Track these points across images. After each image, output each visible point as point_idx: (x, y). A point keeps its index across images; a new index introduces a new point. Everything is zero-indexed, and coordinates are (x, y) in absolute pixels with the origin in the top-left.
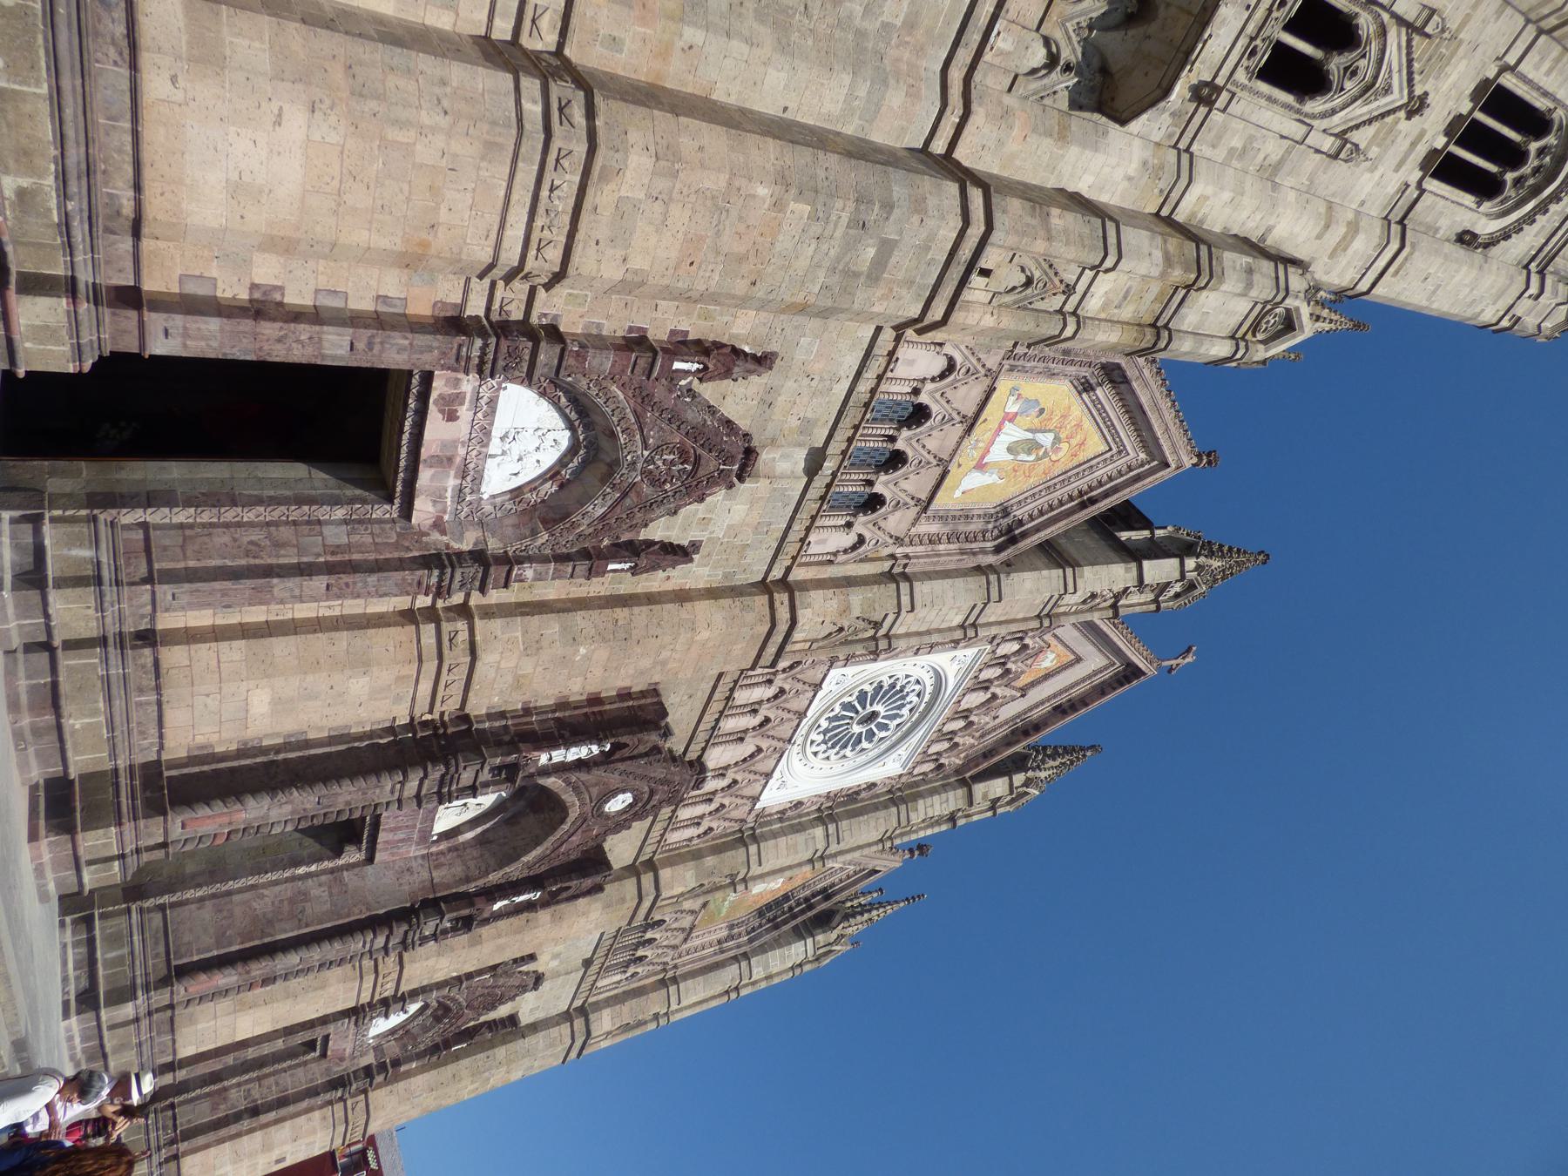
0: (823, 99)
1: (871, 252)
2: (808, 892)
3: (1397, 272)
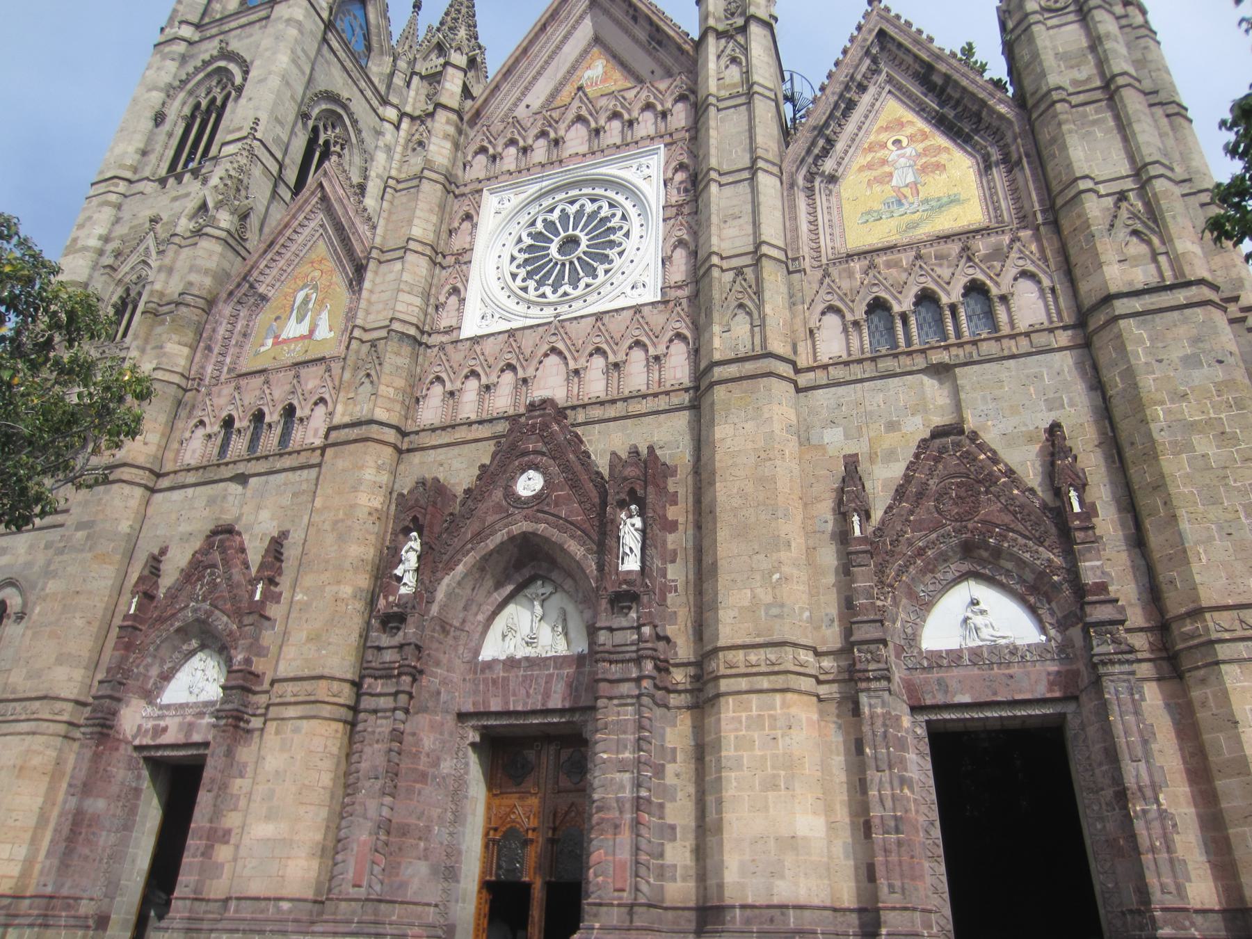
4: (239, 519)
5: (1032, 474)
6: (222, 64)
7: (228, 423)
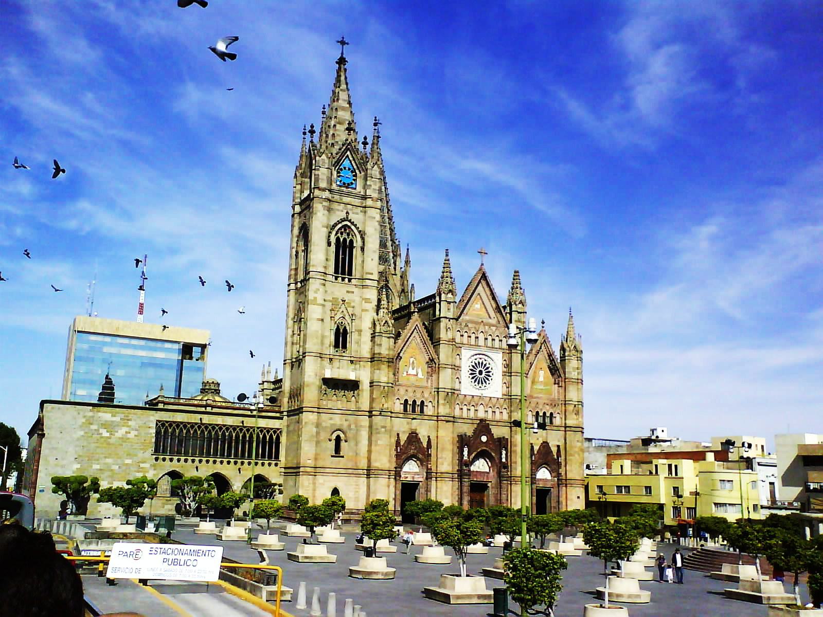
0: (364, 434)
1: (383, 429)
2: (549, 361)
3: (372, 274)
4: (416, 430)
5: (555, 453)
6: (349, 224)
7: (406, 401)
